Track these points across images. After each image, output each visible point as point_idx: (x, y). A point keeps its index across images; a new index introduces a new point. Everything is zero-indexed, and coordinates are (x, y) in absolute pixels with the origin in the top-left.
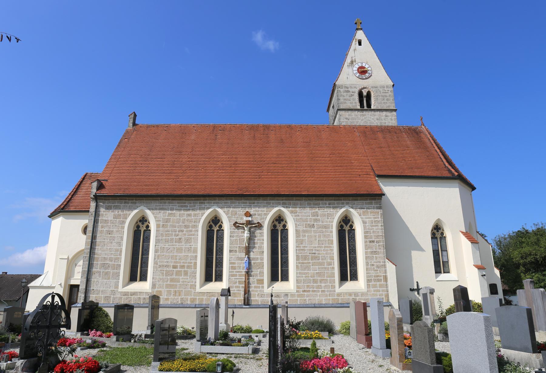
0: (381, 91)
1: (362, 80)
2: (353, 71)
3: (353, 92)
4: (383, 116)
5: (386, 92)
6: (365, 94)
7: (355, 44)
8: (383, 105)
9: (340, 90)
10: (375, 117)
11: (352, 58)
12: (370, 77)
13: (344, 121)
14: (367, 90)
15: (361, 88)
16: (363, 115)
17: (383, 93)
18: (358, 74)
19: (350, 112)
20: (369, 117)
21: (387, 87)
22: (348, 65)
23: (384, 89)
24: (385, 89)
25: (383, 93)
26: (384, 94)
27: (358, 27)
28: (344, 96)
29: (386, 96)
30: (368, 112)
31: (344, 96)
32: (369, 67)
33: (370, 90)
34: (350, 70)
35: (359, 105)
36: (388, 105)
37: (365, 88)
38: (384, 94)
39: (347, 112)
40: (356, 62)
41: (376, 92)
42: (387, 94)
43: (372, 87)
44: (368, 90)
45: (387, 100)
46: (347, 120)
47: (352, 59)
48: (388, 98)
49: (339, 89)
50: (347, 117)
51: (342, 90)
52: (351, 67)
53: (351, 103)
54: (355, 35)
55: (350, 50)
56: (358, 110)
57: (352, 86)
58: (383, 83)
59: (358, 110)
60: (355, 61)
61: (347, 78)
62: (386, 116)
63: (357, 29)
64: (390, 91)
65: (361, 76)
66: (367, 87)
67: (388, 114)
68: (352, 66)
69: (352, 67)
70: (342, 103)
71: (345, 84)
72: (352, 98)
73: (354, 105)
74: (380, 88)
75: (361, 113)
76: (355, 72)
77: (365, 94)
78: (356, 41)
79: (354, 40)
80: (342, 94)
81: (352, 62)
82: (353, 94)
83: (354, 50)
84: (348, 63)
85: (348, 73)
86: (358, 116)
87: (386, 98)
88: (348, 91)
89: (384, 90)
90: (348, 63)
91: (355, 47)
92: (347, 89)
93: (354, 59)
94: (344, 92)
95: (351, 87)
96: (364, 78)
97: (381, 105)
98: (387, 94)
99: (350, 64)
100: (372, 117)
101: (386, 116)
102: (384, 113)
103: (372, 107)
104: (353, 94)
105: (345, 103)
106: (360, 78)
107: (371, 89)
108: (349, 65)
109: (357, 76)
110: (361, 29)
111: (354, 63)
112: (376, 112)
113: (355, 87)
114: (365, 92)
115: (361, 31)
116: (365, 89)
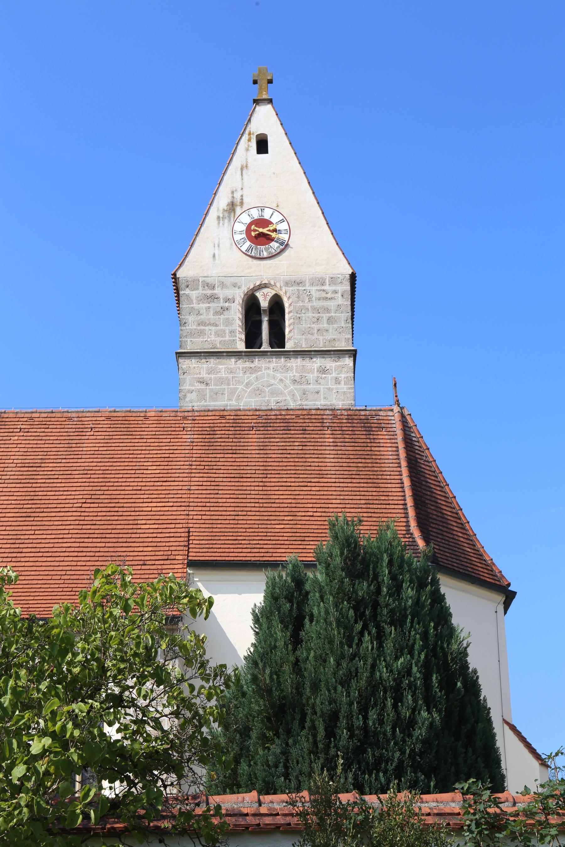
0: (313, 293)
1: (258, 262)
2: (233, 232)
3: (227, 300)
4: (312, 371)
5: (329, 296)
6: (264, 304)
7: (247, 150)
8: (316, 336)
9: (188, 296)
10: (290, 374)
11: (233, 192)
12: (282, 251)
13: (194, 388)
14: (270, 293)
15: (252, 287)
16: (253, 370)
17: (319, 299)
18: (248, 243)
19: (213, 362)
20: (268, 375)
21: (333, 280)
22: (219, 217)
23: (323, 288)
24: (326, 287)
25: (319, 299)
26: (322, 303)
27: (260, 93)
28: (199, 313)
29: (327, 310)
30: (268, 360)
31: (199, 313)
32: (282, 221)
33: (281, 293)
34: (225, 231)
35: (241, 339)
36: (329, 336)
37: (265, 286)
38: (322, 303)
39: (204, 360)
40: (245, 207)
41: (298, 297)
42: (332, 304)
43: (287, 284)
44: (273, 292)
45: (330, 320)
46: (203, 386)
47: (233, 197)
48: (333, 314)
49: (187, 291)
50: (204, 375)
51: (194, 294)
52: (226, 221)
53: (217, 334)
54: (250, 120)
55: (230, 168)
56: (237, 354)
57: (228, 281)
58: (319, 271)
59: (237, 354)
60: (242, 203)
61: (214, 256)
62: (323, 371)
63: (257, 102)
64: (339, 295)
65: (256, 249)
66: (272, 283)
67: (329, 363)
68: (229, 217)
69: (230, 220)
70: (191, 334)
71: (205, 275)
72: (222, 317)
73: (227, 338)
74: (312, 284)
75: (248, 364)
76: (237, 237)
77: (264, 304)
78: (249, 140)
79: (245, 137)
80: (195, 305)
81: (232, 207)
82: (227, 305)
83: (242, 169)
84: (218, 210)
85: (216, 243)
86: (235, 373)
87: (325, 316)
88: (213, 298)
89: (324, 291)
90: (221, 209)
91: (247, 159)
92: (209, 292)
93: (237, 196)
94: (199, 301)
95: (223, 285)
96: (265, 254)
97: (310, 336)
98: (332, 304)
99: (226, 214)
100: (279, 376)
101: (323, 371)
102: (318, 362)
103: (289, 346)
104: (227, 305)
105: (201, 333)
106: (253, 254)
107: (284, 289)
108: (221, 216)
109: (244, 248)
110: (270, 101)
111: (238, 210)
112: (293, 360)
113: (235, 285)
114: (265, 300)
115: (269, 106)
116: (265, 291)
